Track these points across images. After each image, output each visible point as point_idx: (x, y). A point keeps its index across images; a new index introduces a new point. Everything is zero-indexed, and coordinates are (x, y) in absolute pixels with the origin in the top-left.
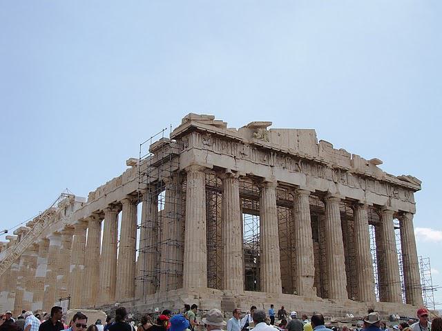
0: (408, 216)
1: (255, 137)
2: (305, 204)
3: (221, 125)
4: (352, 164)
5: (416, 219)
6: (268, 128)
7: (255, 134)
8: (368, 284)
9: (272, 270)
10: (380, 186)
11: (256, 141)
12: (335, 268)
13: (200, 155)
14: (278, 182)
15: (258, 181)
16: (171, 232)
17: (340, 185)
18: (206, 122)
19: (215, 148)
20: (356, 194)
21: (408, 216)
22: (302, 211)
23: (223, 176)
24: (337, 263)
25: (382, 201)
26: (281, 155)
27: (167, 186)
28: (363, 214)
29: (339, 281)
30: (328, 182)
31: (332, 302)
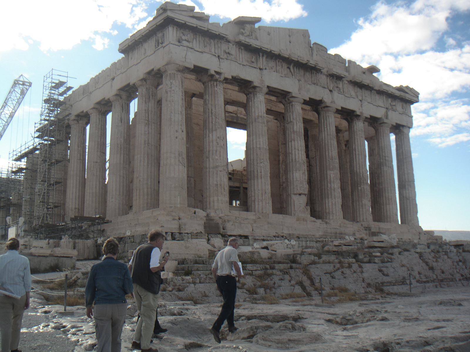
0: (405, 130)
1: (242, 34)
2: (297, 114)
3: (203, 18)
5: (413, 133)
6: (257, 26)
7: (242, 30)
8: (363, 202)
9: (262, 188)
10: (377, 97)
11: (242, 38)
12: (329, 185)
14: (268, 87)
15: (245, 85)
16: (145, 144)
19: (195, 44)
20: (352, 105)
21: (405, 130)
22: (295, 121)
23: (205, 78)
24: (332, 180)
25: (379, 113)
26: (271, 56)
27: (140, 90)
28: (360, 126)
29: (334, 202)
31: (326, 223)
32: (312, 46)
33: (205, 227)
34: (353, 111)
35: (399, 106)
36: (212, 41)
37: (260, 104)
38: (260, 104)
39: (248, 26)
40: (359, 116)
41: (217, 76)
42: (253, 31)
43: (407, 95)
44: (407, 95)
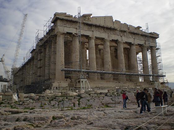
1: (85, 20)
4: (129, 29)
6: (91, 16)
11: (84, 21)
13: (62, 28)
17: (123, 37)
18: (62, 15)
20: (131, 40)
25: (142, 43)
26: (96, 26)
30: (117, 36)
32: (114, 21)
33: (68, 85)
34: (131, 43)
35: (151, 40)
36: (74, 23)
37: (93, 43)
38: (93, 43)
39: (87, 17)
40: (133, 44)
41: (76, 35)
42: (89, 19)
43: (153, 36)
44: (153, 36)
